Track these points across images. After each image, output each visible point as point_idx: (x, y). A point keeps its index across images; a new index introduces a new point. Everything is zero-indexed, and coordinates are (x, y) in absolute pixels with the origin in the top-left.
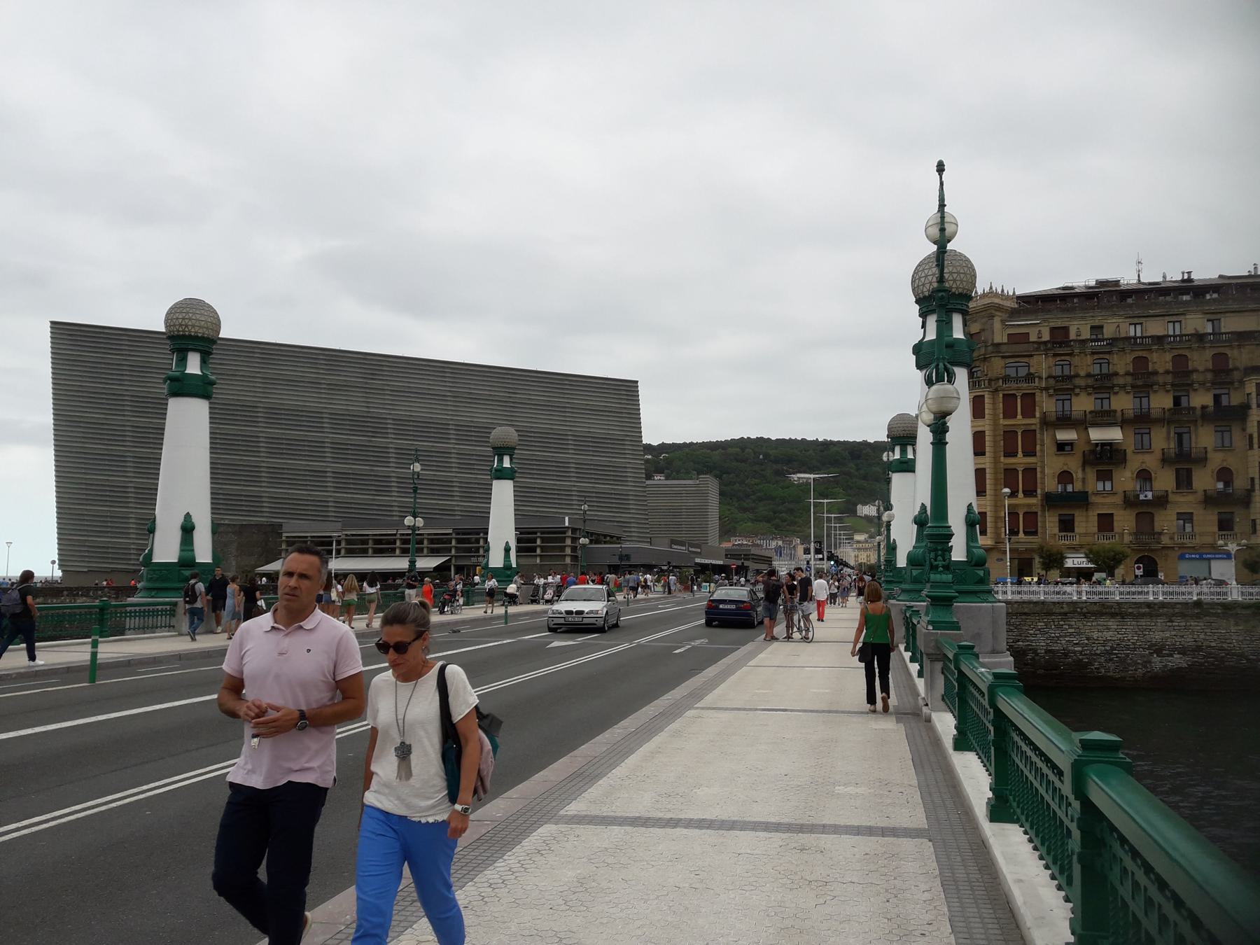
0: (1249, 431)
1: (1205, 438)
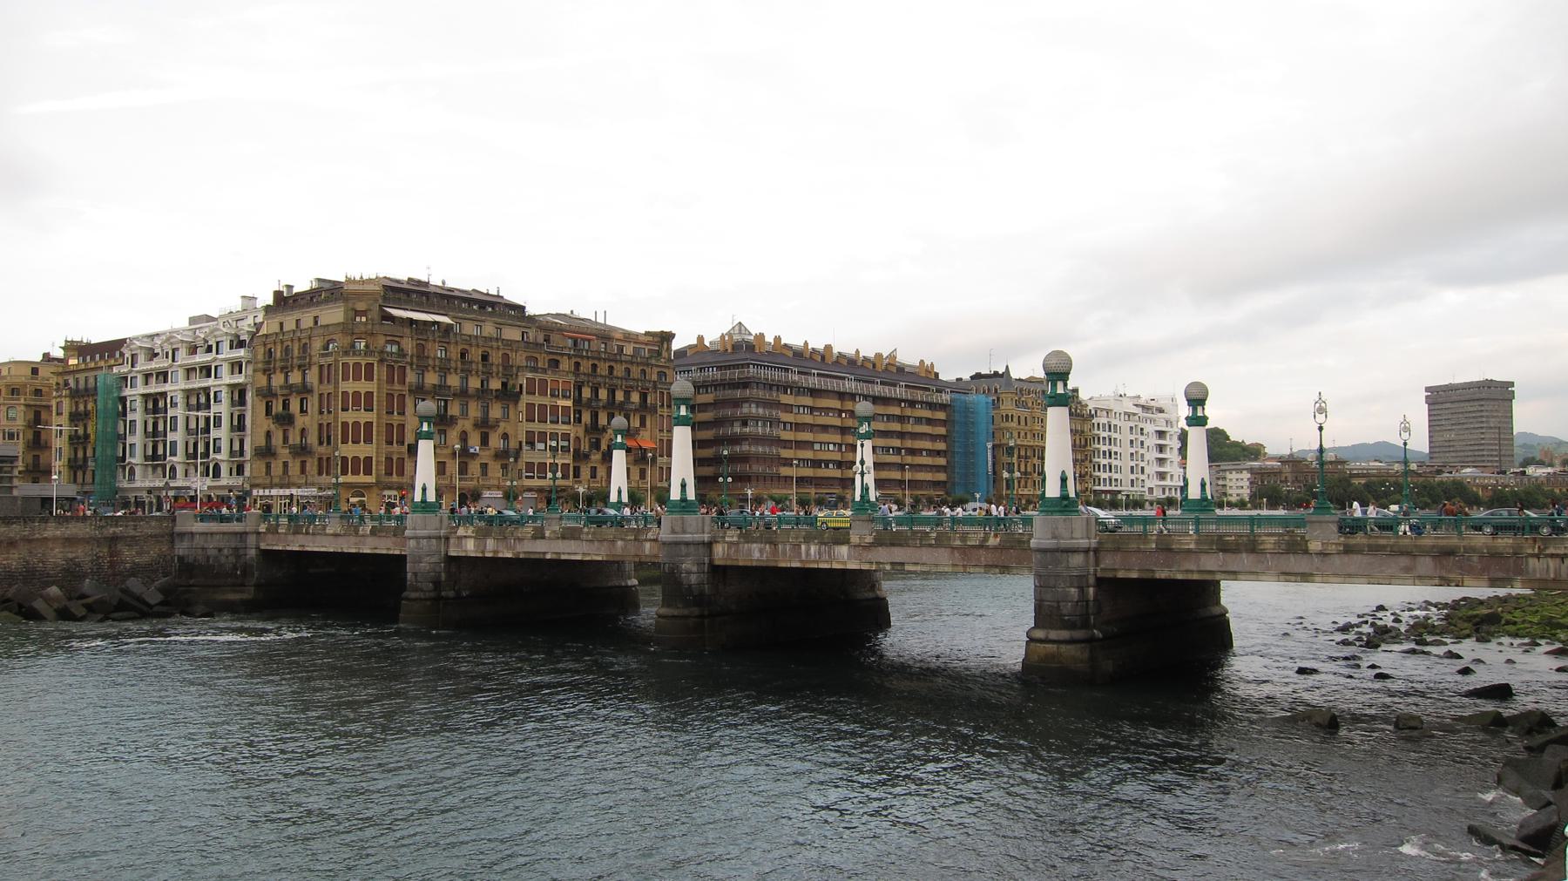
0: (520, 409)
1: (496, 412)
